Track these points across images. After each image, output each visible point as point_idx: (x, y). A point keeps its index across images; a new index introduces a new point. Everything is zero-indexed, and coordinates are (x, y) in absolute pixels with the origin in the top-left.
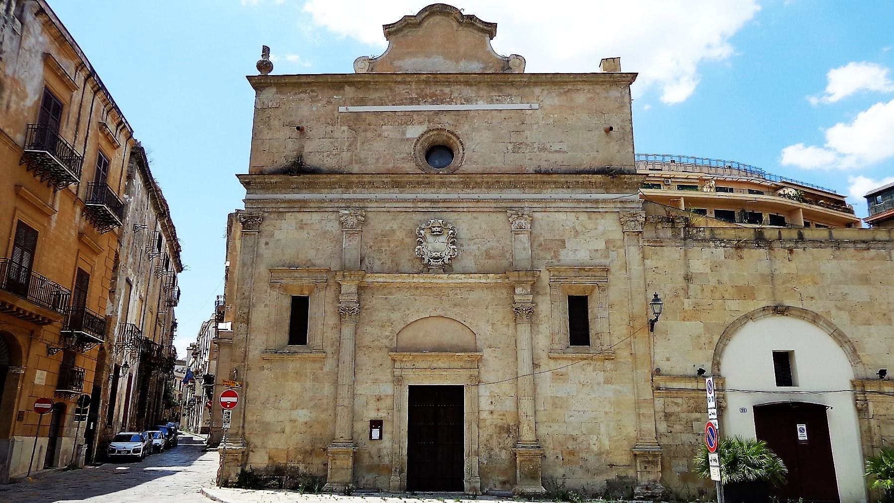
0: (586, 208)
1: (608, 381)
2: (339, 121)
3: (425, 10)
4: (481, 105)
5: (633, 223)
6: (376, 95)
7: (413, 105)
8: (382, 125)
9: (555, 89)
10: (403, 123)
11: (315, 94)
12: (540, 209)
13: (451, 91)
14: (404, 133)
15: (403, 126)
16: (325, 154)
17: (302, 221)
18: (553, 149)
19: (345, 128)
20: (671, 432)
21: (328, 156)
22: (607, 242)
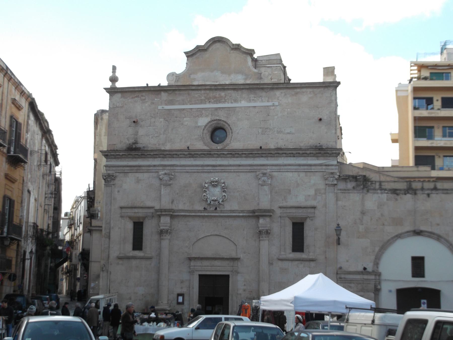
0: (304, 169)
2: (158, 115)
3: (210, 40)
4: (244, 104)
5: (332, 179)
6: (180, 98)
7: (202, 104)
8: (184, 117)
10: (196, 116)
11: (144, 98)
12: (277, 170)
13: (225, 95)
14: (197, 123)
15: (196, 118)
16: (151, 136)
17: (138, 178)
18: (286, 131)
19: (162, 120)
21: (152, 138)
22: (316, 190)
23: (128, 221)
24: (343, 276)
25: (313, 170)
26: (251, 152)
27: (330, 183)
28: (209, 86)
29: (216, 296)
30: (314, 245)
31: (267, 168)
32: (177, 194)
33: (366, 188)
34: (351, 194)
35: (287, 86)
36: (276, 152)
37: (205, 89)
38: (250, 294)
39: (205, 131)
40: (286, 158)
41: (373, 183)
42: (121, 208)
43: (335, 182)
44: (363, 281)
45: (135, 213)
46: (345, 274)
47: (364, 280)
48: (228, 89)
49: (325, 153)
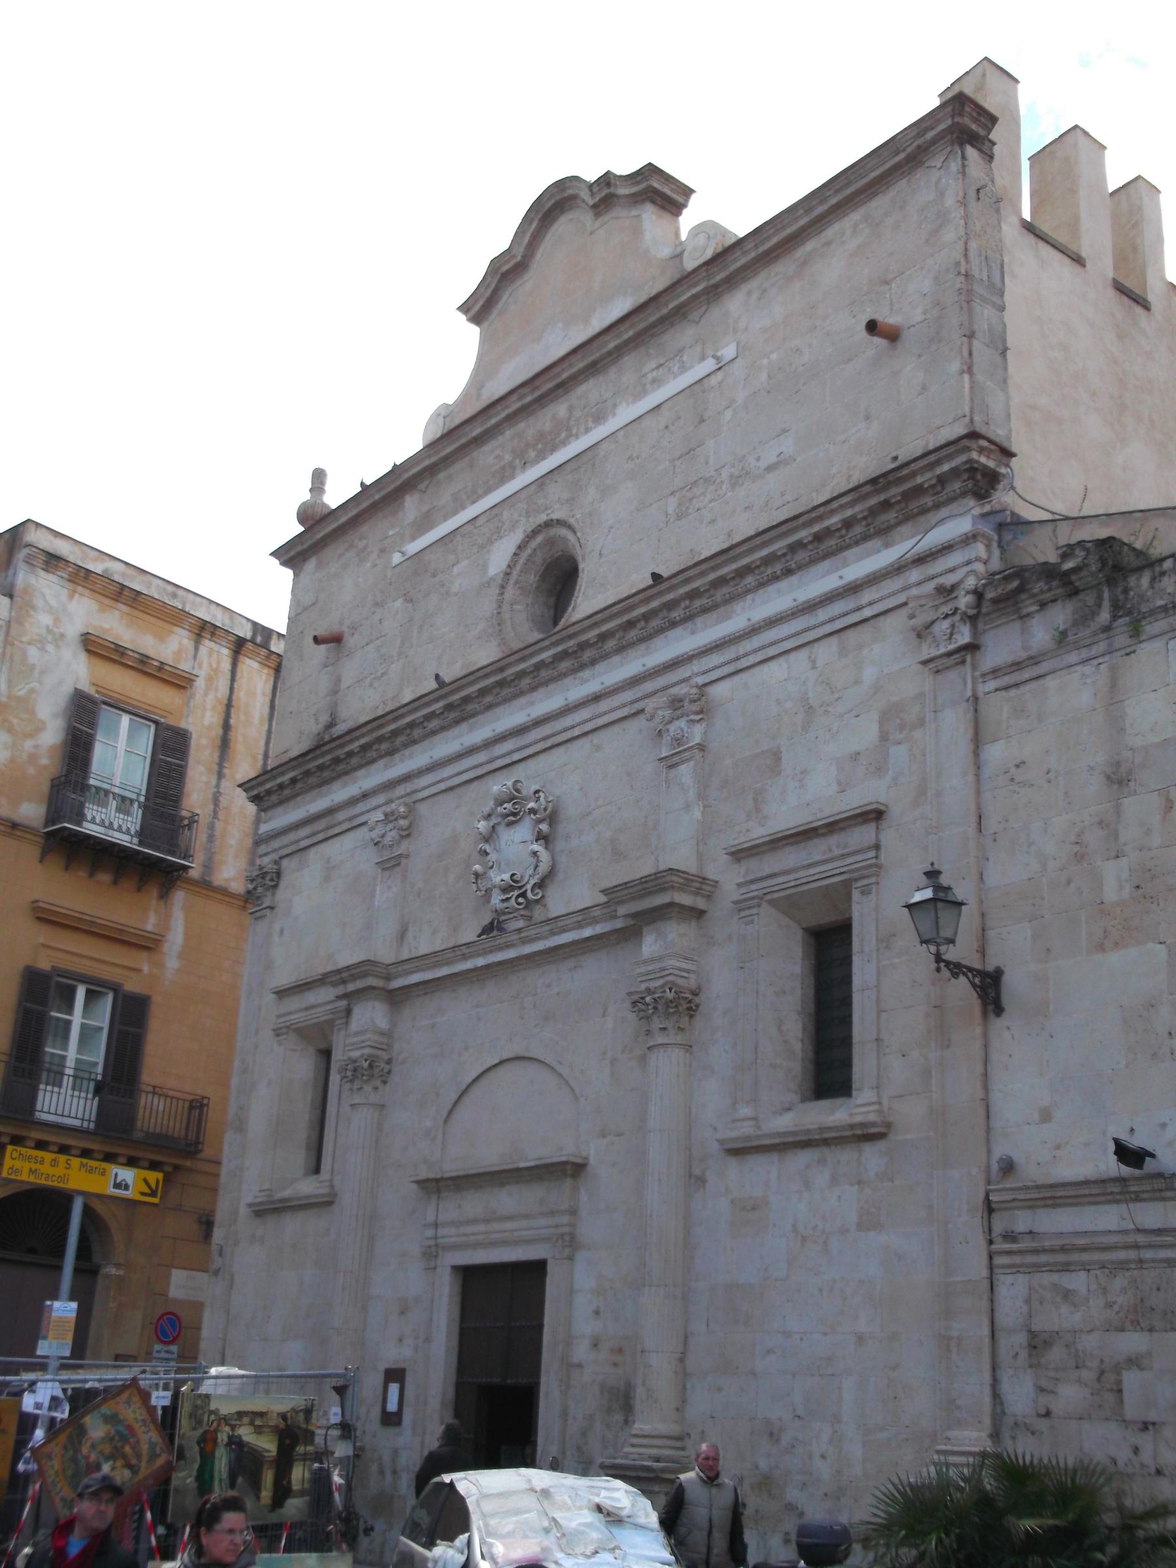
0: (832, 620)
1: (869, 1222)
3: (527, 219)
4: (626, 413)
6: (445, 497)
9: (777, 274)
13: (571, 409)
18: (763, 464)
19: (399, 603)
20: (1048, 1414)
21: (371, 685)
23: (293, 1050)
24: (1022, 1221)
25: (867, 613)
26: (626, 618)
27: (942, 650)
28: (514, 397)
29: (509, 1381)
30: (878, 1040)
31: (687, 674)
32: (419, 895)
33: (1129, 613)
34: (1051, 683)
35: (761, 250)
36: (712, 576)
37: (511, 418)
38: (615, 1365)
39: (510, 593)
40: (761, 591)
41: (1163, 574)
42: (282, 993)
43: (964, 636)
44: (1137, 1247)
45: (307, 1009)
46: (1032, 1205)
47: (1141, 1239)
48: (575, 380)
49: (907, 496)
